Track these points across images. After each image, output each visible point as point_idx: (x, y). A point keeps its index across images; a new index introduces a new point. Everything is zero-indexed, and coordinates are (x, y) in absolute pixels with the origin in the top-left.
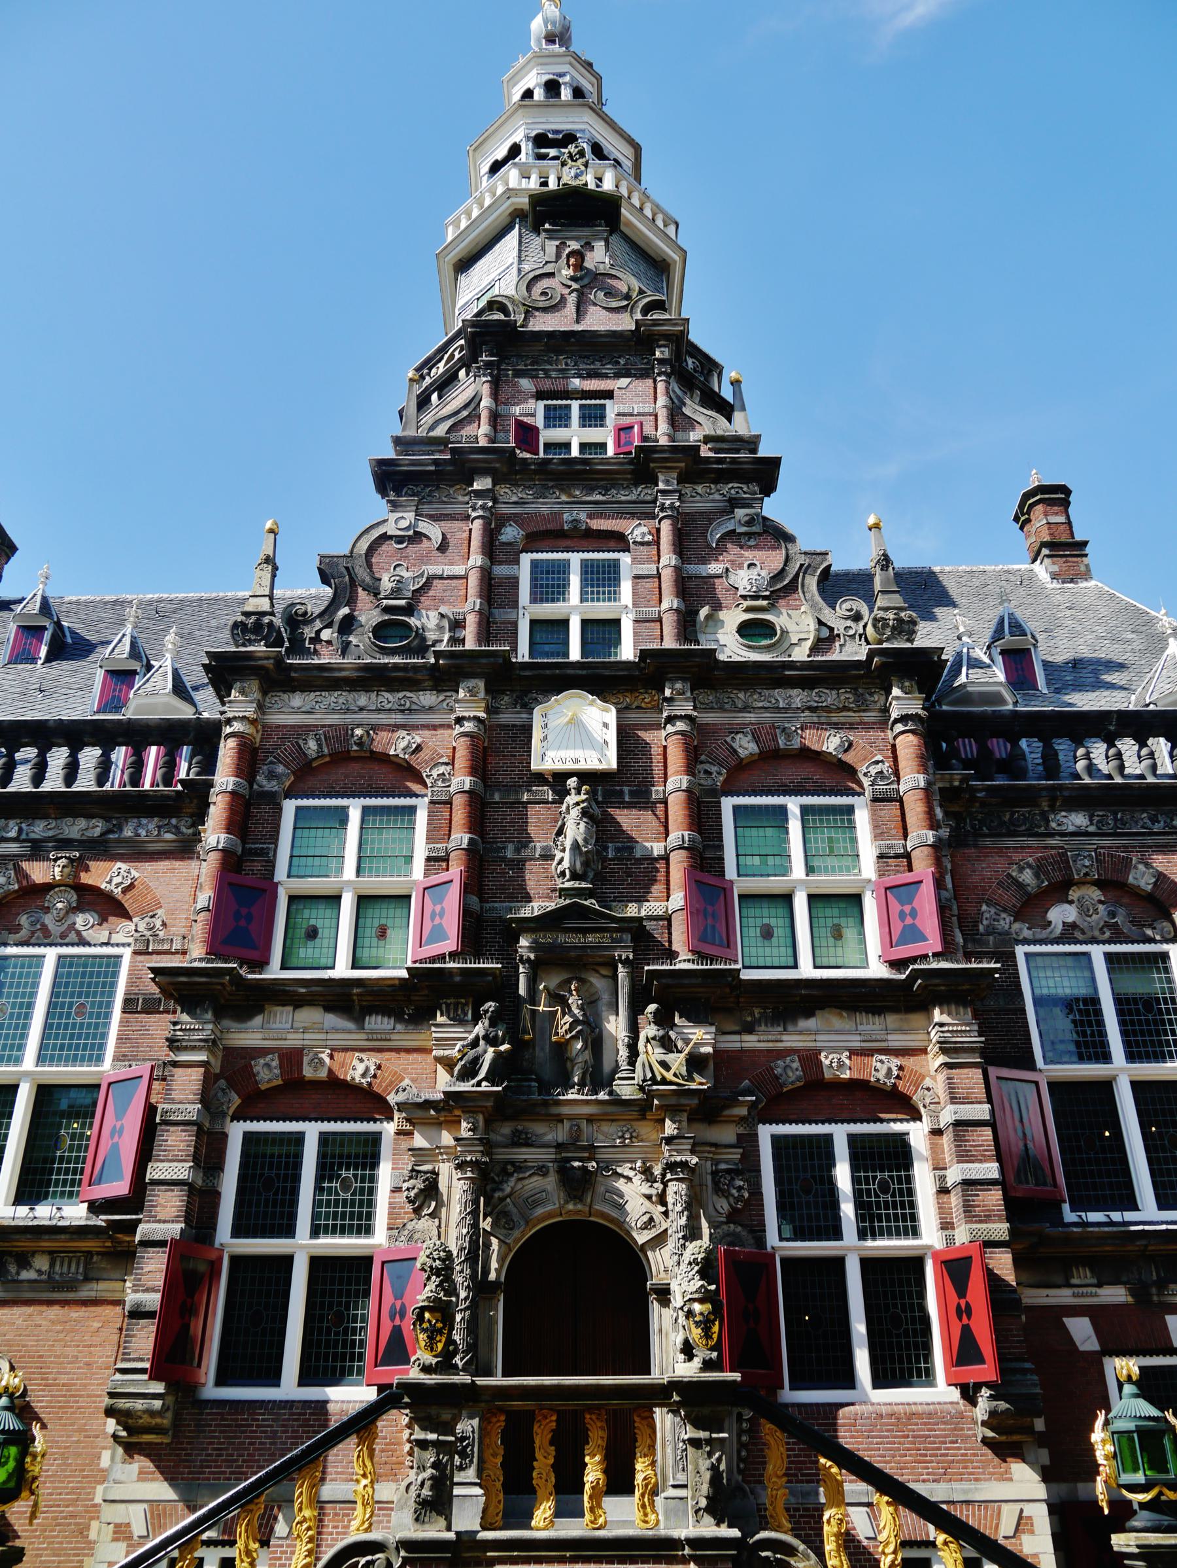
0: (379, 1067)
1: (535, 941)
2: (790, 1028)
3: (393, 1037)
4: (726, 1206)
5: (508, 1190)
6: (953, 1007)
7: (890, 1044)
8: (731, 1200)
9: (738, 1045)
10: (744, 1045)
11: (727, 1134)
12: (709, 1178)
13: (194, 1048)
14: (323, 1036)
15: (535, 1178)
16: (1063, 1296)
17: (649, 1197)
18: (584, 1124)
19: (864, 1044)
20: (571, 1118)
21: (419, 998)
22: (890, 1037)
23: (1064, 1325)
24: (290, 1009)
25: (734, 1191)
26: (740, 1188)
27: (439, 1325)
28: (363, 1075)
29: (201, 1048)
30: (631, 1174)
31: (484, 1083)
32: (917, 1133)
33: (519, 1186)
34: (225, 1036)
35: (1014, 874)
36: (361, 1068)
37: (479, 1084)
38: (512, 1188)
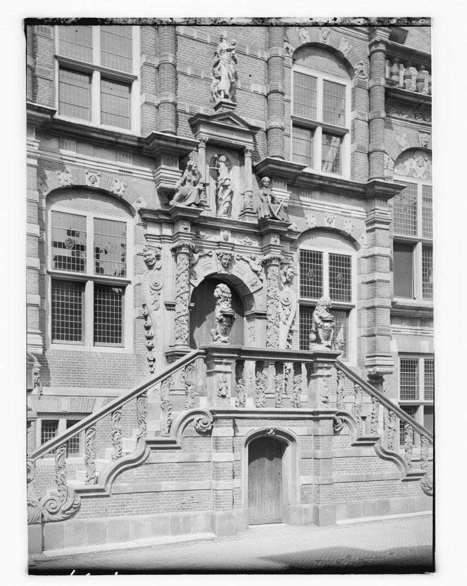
0: (126, 187)
8: (288, 277)
10: (295, 205)
17: (256, 272)
18: (229, 234)
28: (119, 190)
30: (249, 259)
31: (193, 205)
32: (355, 256)
35: (398, 140)
37: (190, 205)
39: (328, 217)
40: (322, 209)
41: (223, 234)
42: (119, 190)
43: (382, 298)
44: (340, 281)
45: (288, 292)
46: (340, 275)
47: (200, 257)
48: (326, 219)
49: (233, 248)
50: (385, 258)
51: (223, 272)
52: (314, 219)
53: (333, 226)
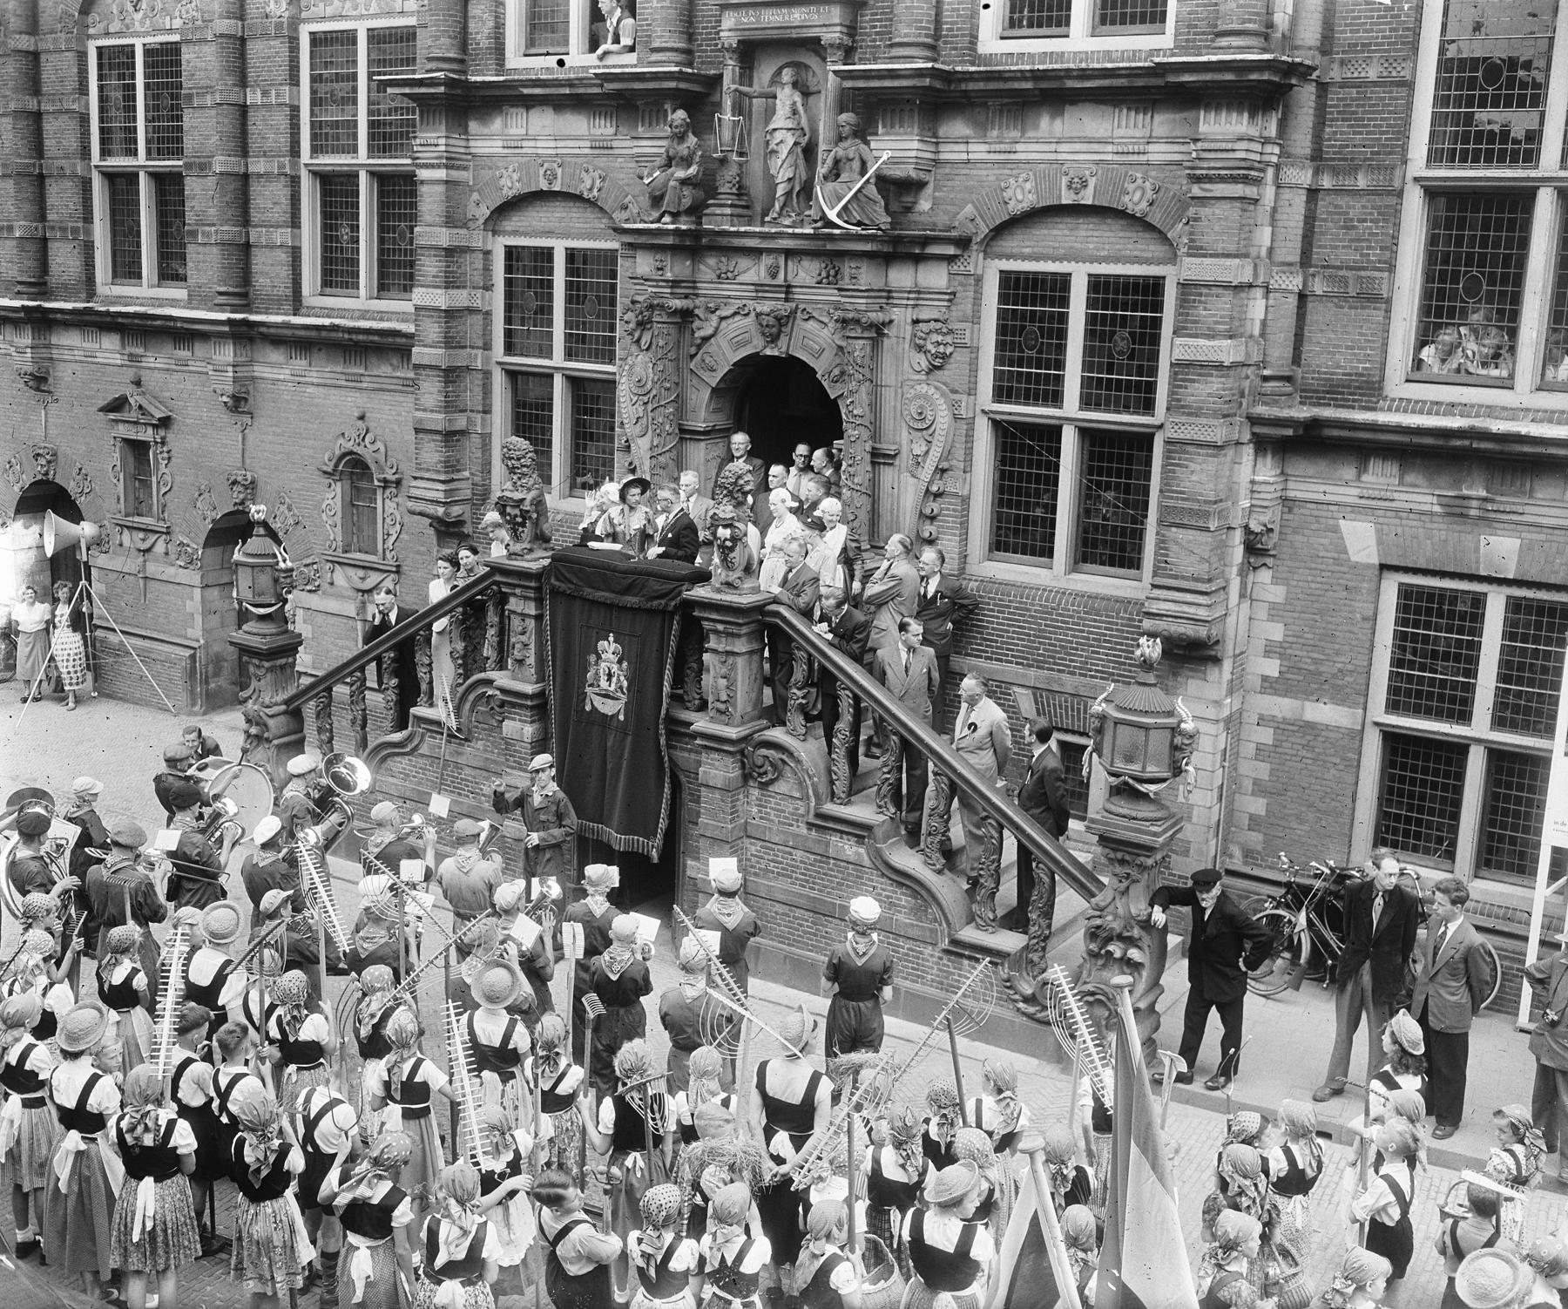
0: (603, 179)
1: (738, 22)
2: (1031, 134)
3: (615, 144)
4: (924, 364)
5: (710, 331)
6: (1224, 114)
7: (1151, 157)
9: (964, 156)
10: (971, 156)
11: (935, 277)
12: (909, 328)
13: (432, 166)
14: (552, 144)
15: (737, 318)
16: (1349, 494)
19: (1116, 158)
20: (770, 251)
21: (623, 101)
22: (1151, 148)
23: (1336, 529)
24: (522, 111)
25: (930, 347)
26: (939, 344)
27: (519, 520)
28: (591, 189)
29: (439, 166)
33: (724, 324)
34: (472, 143)
36: (588, 184)
38: (717, 329)
39: (1071, 174)
40: (1053, 156)
41: (767, 260)
42: (591, 189)
43: (1189, 414)
44: (1121, 353)
45: (926, 397)
46: (1122, 340)
47: (722, 319)
48: (1064, 180)
49: (787, 293)
50: (1215, 291)
51: (768, 352)
52: (1028, 186)
53: (1087, 198)
